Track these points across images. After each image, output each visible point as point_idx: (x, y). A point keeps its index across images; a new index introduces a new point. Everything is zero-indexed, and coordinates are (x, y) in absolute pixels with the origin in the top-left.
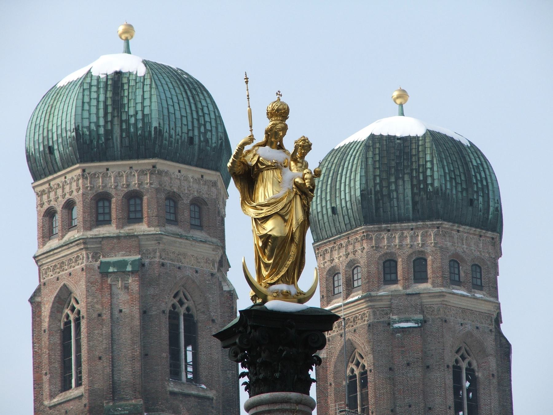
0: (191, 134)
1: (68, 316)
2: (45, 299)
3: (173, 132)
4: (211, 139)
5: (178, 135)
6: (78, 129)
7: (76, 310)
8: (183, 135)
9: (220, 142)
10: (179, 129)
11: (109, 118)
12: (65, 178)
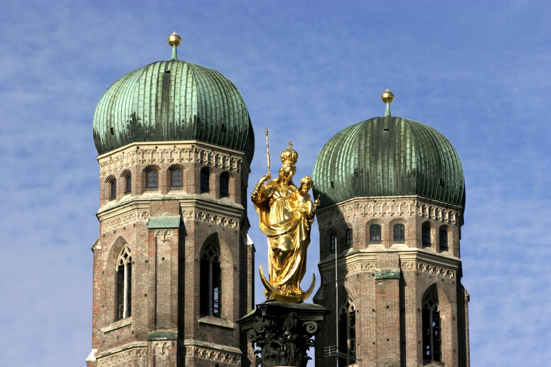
0: (223, 122)
1: (122, 261)
2: (104, 248)
3: (209, 120)
4: (239, 126)
5: (213, 122)
6: (135, 115)
7: (128, 256)
8: (217, 122)
9: (245, 128)
10: (214, 118)
11: (159, 108)
12: (123, 153)
